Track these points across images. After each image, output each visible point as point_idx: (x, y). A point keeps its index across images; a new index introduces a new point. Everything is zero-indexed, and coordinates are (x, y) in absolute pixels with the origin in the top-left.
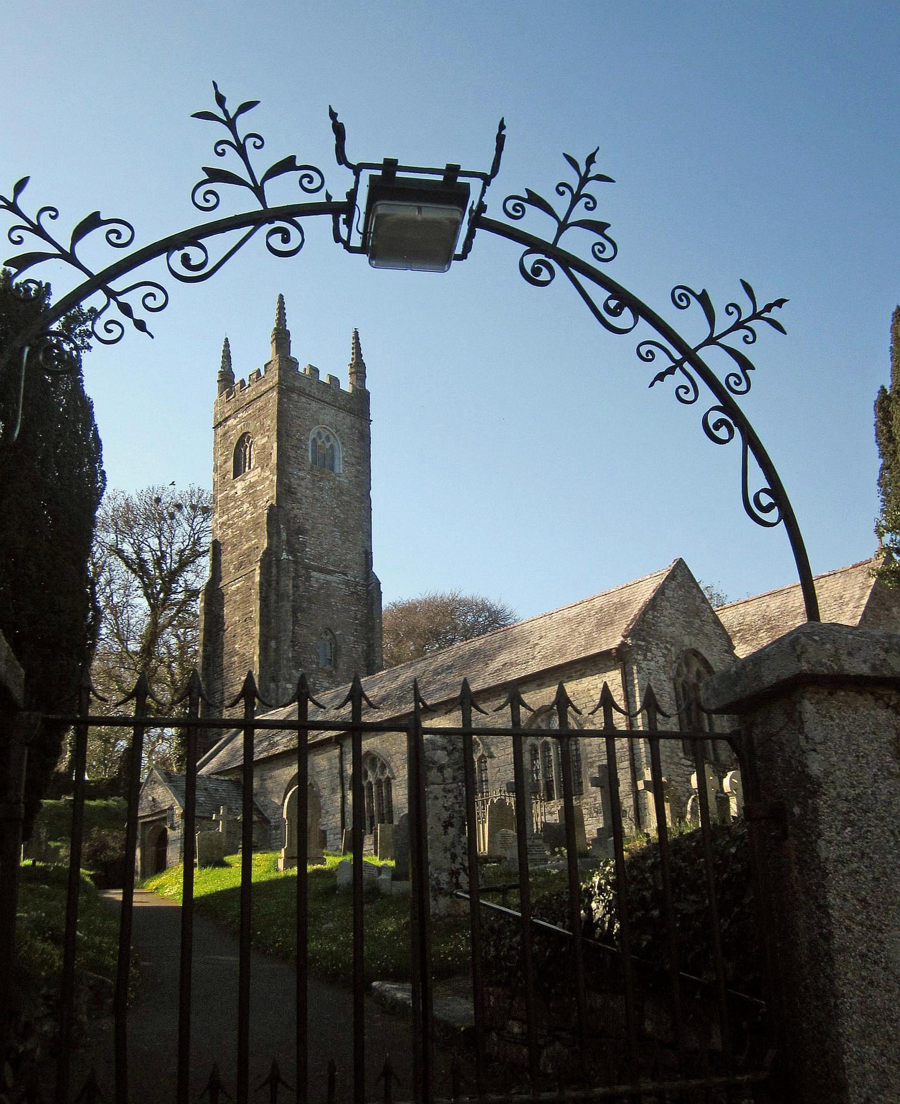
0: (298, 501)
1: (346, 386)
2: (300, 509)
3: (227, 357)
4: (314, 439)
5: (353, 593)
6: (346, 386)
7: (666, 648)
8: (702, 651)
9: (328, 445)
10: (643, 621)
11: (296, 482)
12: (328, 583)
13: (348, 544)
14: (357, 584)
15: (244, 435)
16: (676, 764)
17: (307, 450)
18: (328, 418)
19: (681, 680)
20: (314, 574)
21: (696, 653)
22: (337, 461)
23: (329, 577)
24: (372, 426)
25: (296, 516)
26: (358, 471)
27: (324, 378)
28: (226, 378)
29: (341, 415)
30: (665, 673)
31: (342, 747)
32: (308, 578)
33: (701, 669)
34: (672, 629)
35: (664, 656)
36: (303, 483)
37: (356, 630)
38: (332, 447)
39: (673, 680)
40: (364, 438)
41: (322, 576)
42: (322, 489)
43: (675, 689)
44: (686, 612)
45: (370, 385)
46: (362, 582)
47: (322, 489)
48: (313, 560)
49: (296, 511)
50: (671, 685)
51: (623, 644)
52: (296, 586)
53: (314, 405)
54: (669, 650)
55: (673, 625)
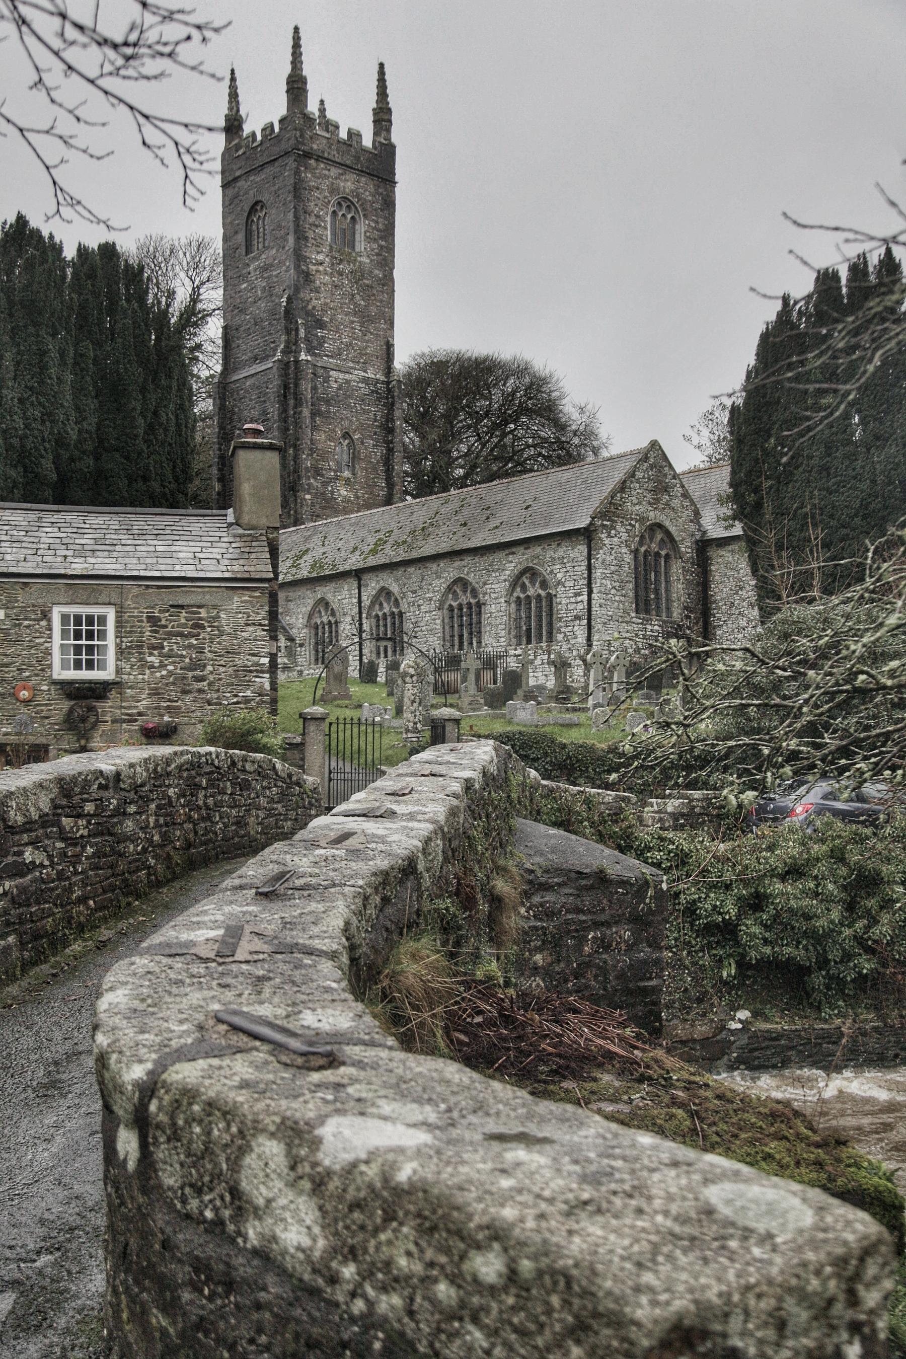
0: (317, 291)
1: (367, 141)
2: (319, 299)
3: (234, 96)
4: (334, 212)
5: (373, 392)
6: (367, 141)
7: (630, 524)
8: (667, 523)
9: (349, 216)
10: (611, 503)
11: (314, 268)
12: (348, 382)
13: (369, 336)
14: (377, 381)
15: (257, 203)
16: (627, 622)
17: (326, 228)
18: (349, 186)
19: (643, 549)
20: (332, 373)
21: (660, 526)
22: (357, 236)
23: (347, 376)
24: (398, 189)
25: (314, 308)
26: (381, 247)
27: (343, 135)
28: (233, 125)
29: (363, 179)
30: (627, 546)
31: (359, 580)
32: (327, 380)
33: (665, 538)
34: (637, 507)
35: (628, 531)
36: (321, 268)
37: (375, 434)
38: (353, 218)
39: (636, 552)
40: (389, 205)
41: (341, 376)
42: (340, 274)
43: (636, 558)
44: (654, 491)
45: (397, 136)
46: (383, 378)
47: (340, 274)
48: (331, 357)
49: (314, 302)
50: (632, 556)
51: (591, 524)
52: (314, 388)
53: (334, 172)
54: (634, 526)
55: (640, 503)
